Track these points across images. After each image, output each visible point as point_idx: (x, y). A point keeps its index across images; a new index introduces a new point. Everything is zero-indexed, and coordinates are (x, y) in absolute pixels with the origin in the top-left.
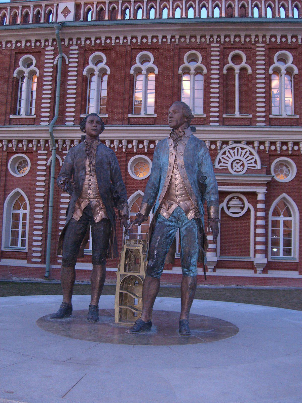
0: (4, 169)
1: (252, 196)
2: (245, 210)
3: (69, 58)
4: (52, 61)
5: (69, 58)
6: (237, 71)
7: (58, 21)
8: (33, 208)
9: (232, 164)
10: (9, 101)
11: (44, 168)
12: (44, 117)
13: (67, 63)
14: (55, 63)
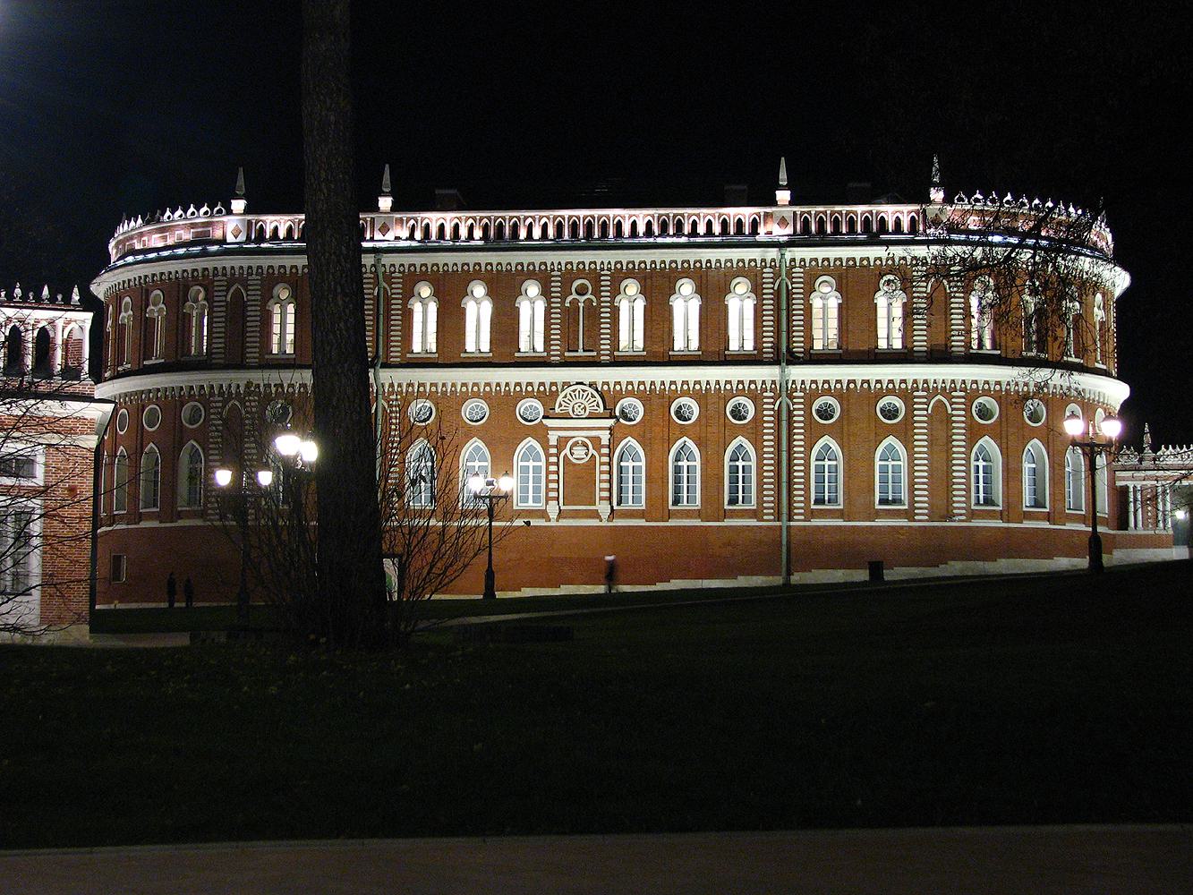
1: (596, 441)
2: (589, 456)
6: (581, 305)
9: (573, 407)
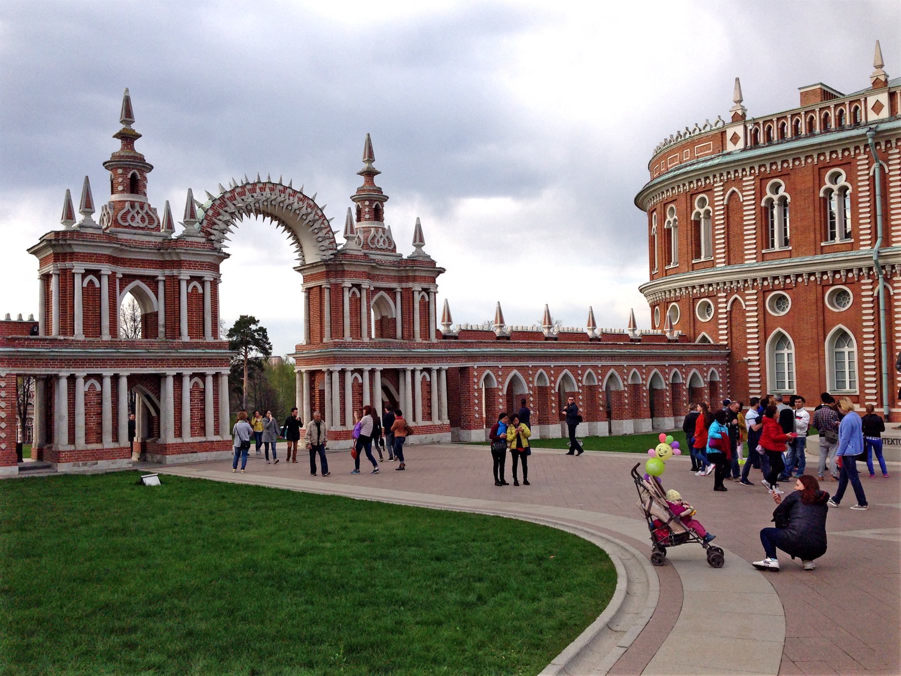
0: (820, 304)
3: (889, 165)
4: (867, 172)
5: (889, 165)
7: (870, 119)
8: (860, 347)
10: (818, 227)
11: (871, 299)
12: (864, 240)
13: (887, 171)
14: (871, 174)
